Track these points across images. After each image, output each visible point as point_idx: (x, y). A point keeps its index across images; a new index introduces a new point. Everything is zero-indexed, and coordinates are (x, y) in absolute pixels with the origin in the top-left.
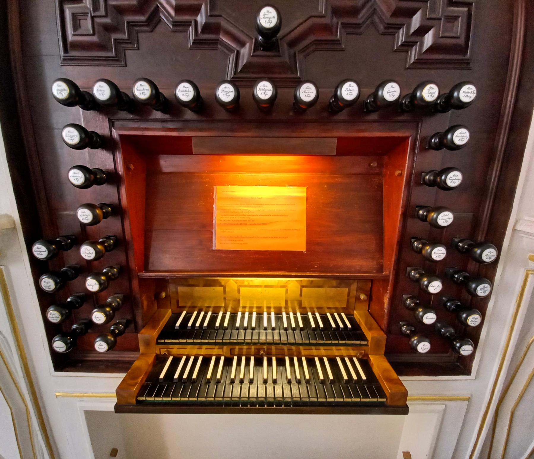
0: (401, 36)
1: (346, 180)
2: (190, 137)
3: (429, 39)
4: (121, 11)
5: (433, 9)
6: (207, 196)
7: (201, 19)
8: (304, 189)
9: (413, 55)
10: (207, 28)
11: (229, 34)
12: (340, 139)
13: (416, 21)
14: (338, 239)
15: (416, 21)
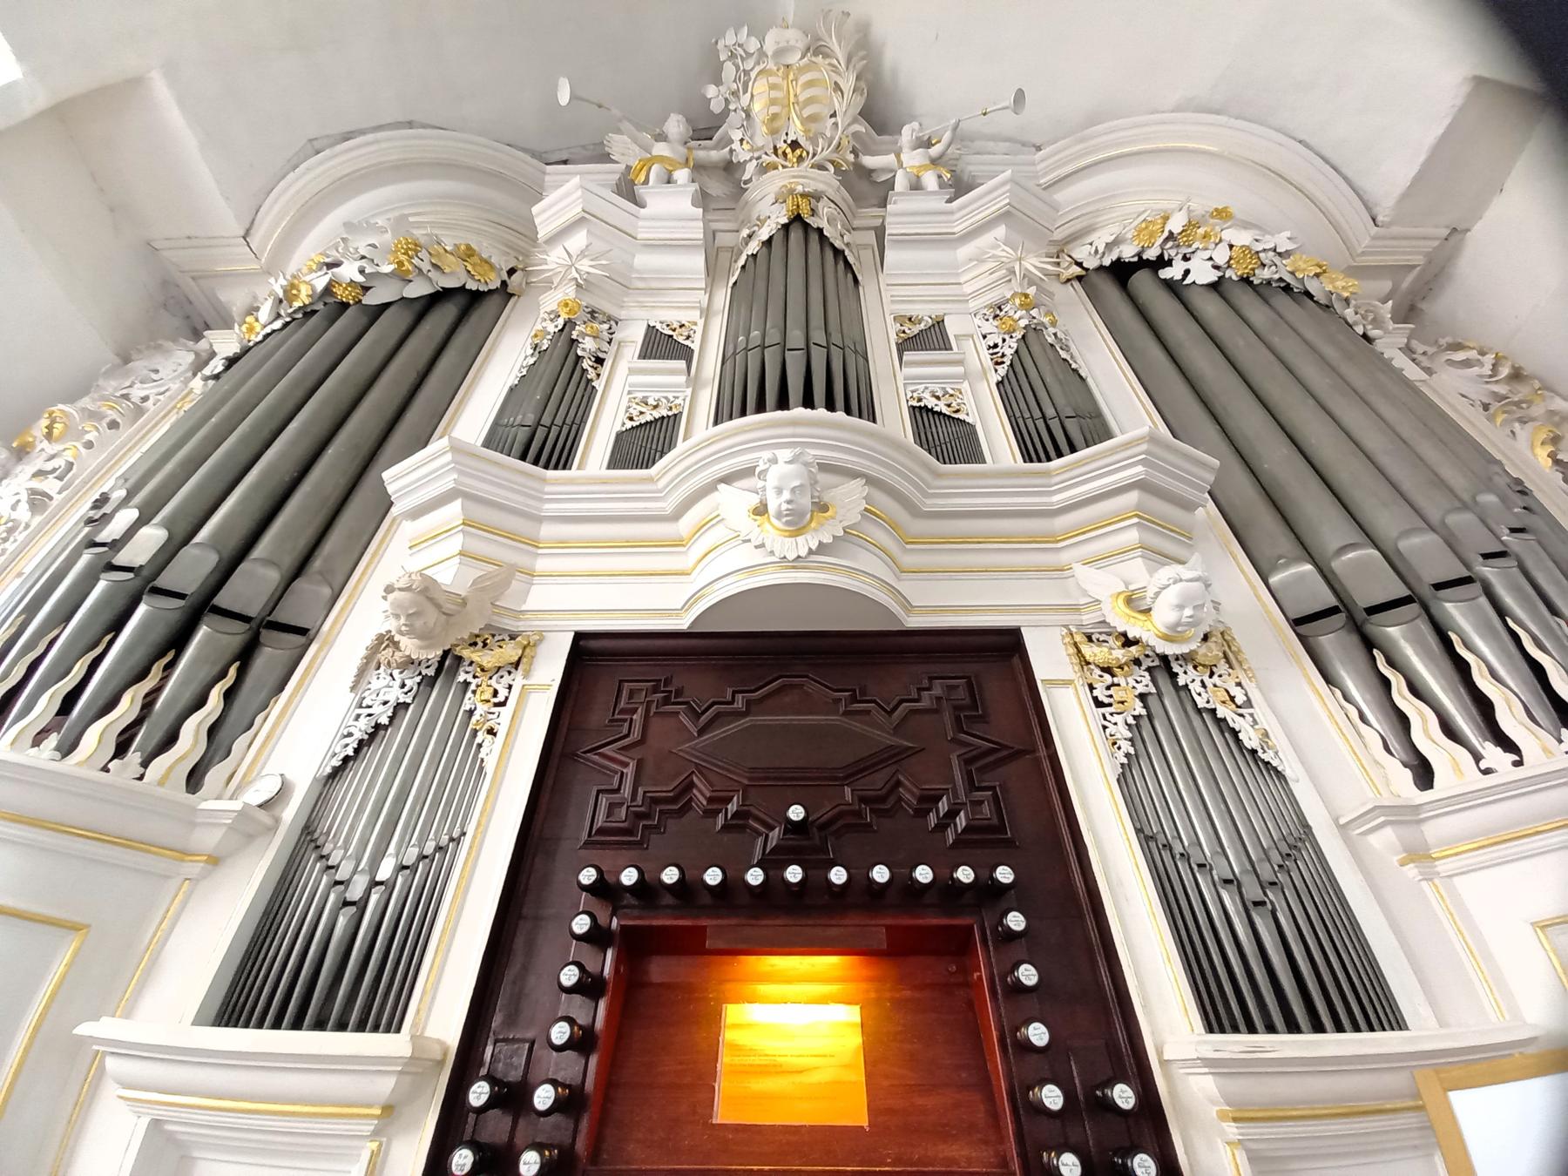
0: (932, 819)
1: (917, 995)
2: (705, 927)
3: (961, 821)
4: (655, 801)
5: (956, 795)
6: (714, 1021)
7: (732, 807)
8: (857, 1009)
9: (950, 837)
10: (735, 815)
11: (757, 819)
12: (888, 927)
13: (943, 806)
14: (920, 1101)
15: (943, 806)
